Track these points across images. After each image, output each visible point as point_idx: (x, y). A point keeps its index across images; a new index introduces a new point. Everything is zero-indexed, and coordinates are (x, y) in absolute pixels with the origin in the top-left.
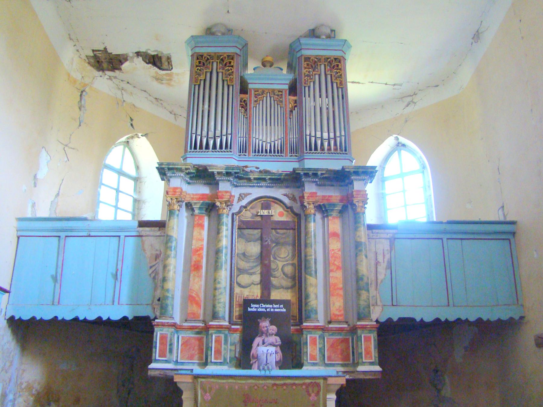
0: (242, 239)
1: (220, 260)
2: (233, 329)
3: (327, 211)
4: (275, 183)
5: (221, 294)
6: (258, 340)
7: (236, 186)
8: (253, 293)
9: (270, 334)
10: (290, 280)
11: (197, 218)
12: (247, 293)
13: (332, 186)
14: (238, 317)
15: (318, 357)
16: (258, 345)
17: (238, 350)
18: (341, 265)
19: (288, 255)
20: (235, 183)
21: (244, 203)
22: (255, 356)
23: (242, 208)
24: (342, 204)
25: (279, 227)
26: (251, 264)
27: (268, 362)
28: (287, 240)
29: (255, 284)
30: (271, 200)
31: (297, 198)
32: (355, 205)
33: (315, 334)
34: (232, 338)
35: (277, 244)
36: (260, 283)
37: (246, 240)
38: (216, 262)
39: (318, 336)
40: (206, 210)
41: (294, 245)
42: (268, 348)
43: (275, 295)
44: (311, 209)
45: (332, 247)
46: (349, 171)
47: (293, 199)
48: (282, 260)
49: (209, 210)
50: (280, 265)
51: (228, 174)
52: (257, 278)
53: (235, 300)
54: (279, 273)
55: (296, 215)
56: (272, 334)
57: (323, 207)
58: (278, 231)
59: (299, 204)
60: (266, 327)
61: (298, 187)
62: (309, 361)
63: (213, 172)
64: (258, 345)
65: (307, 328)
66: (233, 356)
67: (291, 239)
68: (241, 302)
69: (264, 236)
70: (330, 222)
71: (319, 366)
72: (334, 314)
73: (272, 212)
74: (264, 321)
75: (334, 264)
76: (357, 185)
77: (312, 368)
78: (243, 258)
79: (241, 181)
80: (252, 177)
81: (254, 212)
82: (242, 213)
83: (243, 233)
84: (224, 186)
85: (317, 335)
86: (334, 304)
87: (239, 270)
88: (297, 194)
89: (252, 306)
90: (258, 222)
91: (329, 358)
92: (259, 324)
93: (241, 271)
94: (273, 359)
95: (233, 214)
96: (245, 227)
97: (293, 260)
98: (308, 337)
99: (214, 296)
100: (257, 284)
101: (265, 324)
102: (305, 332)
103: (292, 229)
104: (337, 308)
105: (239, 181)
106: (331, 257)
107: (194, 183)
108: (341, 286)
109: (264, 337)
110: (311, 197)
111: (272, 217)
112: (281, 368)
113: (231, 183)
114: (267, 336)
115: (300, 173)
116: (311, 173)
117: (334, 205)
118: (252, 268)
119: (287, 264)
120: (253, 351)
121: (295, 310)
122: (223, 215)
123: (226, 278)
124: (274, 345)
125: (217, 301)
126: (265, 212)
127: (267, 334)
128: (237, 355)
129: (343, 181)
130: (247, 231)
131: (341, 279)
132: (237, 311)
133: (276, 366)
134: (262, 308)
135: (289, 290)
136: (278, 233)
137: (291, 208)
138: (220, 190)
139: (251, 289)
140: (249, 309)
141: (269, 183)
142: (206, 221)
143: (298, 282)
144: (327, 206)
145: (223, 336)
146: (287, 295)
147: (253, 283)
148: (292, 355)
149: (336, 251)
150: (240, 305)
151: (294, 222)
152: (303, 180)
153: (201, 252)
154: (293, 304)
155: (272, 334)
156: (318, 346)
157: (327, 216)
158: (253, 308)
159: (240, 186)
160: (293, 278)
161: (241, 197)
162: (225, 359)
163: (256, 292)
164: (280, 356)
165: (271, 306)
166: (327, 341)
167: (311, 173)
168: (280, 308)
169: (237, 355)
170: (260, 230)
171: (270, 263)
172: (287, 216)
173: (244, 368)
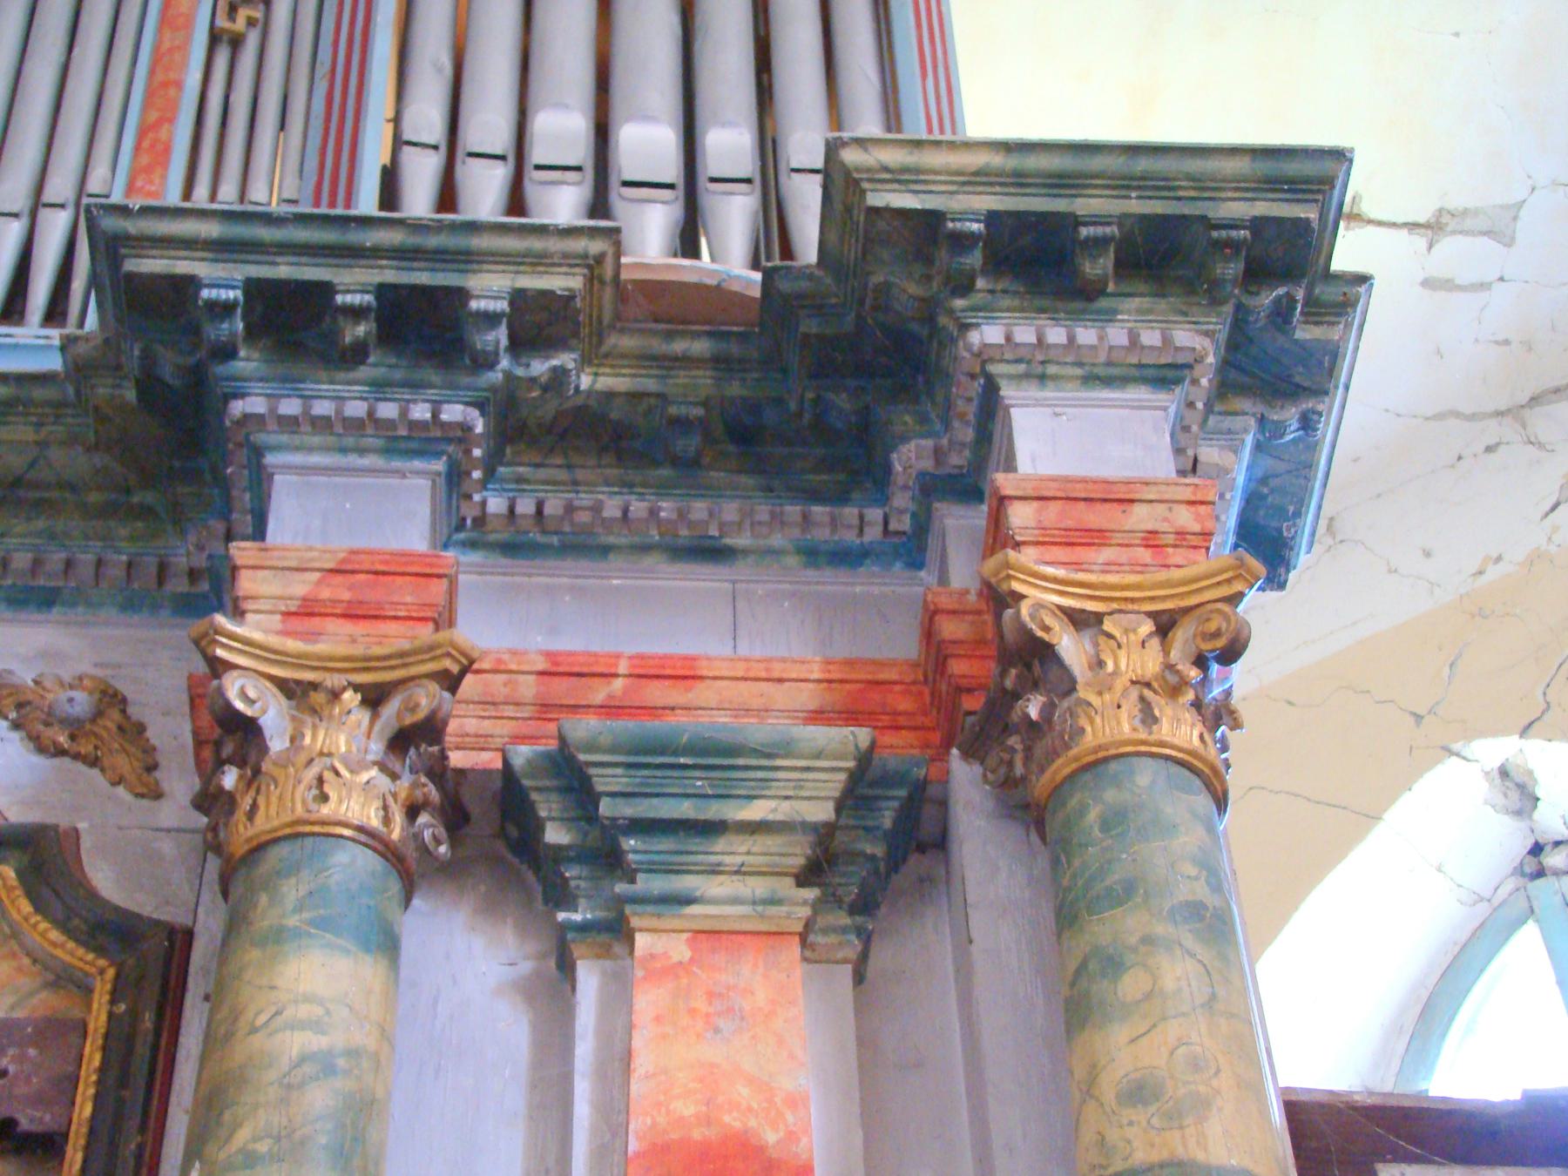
3: (607, 858)
13: (710, 551)
46: (931, 221)
57: (547, 806)
59: (177, 806)
70: (647, 1001)
76: (1062, 436)
110: (352, 614)
115: (189, 284)
116: (354, 285)
117: (719, 759)
129: (855, 464)
144: (604, 781)
151: (59, 1032)
152: (255, 404)
157: (614, 931)
167: (354, 285)
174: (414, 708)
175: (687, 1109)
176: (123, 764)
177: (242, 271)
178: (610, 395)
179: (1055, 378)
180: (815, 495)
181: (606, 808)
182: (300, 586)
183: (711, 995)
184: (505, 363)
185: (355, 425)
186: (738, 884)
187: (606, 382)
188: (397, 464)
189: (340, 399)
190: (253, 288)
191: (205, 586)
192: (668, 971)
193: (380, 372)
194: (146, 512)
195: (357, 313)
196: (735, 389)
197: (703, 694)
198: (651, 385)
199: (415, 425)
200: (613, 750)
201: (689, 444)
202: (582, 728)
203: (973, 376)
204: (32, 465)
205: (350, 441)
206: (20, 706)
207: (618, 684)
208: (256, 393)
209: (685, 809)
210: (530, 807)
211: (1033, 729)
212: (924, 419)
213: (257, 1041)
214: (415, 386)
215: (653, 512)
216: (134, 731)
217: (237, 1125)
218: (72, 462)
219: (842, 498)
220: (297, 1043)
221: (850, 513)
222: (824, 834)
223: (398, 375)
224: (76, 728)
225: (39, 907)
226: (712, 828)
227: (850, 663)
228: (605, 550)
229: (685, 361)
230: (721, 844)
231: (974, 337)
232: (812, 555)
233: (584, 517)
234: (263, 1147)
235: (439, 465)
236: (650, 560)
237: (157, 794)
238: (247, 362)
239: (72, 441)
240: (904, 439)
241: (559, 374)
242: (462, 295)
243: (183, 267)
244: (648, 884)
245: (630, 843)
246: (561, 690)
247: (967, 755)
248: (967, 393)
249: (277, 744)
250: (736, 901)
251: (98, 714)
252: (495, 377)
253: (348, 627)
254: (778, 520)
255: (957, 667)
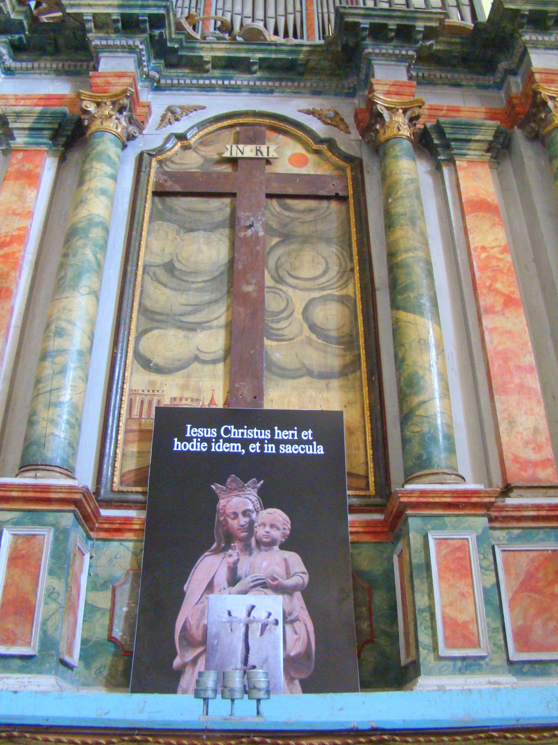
0: (165, 224)
1: (72, 260)
2: (109, 520)
3: (447, 146)
4: (280, 80)
5: (63, 371)
6: (210, 566)
7: (158, 88)
8: (199, 390)
9: (259, 543)
10: (335, 349)
11: (20, 156)
12: (172, 391)
13: (457, 85)
14: (131, 477)
15: (483, 627)
16: (210, 587)
17: (122, 609)
18: (517, 295)
19: (325, 272)
20: (153, 73)
21: (179, 127)
22: (197, 633)
23: (173, 140)
24: (498, 123)
25: (290, 191)
26: (194, 298)
27: (252, 660)
28: (320, 227)
29: (204, 362)
30: (267, 121)
31: (350, 120)
32: (544, 104)
33: (455, 528)
34: (103, 560)
35: (287, 238)
36: (225, 358)
37: (181, 227)
38: (62, 266)
39: (472, 539)
40: (55, 137)
41: (345, 242)
42: (251, 599)
43: (279, 396)
44: (399, 126)
45: (476, 240)
47: (335, 121)
48: (308, 289)
49: (63, 140)
50: (299, 300)
51: (129, 24)
52: (214, 341)
53: (124, 412)
54: (294, 326)
55: (348, 158)
56: (271, 544)
57: (434, 136)
58: (289, 202)
60: (246, 513)
61: (351, 94)
62: (443, 651)
63: (81, 15)
64: (210, 587)
65: (425, 504)
66: (101, 633)
67: (335, 225)
68: (149, 423)
69: (241, 214)
70: (461, 174)
71: (494, 670)
72: (516, 460)
73: (270, 149)
74: (241, 489)
75: (497, 291)
77: (456, 682)
78: (164, 276)
79: (173, 72)
80: (207, 55)
81: (212, 152)
82: (169, 153)
83: (171, 210)
84: (117, 65)
85: (470, 528)
86: (512, 423)
87: (144, 311)
88: (347, 109)
89: (190, 431)
90: (226, 175)
91: (524, 639)
92: (216, 499)
93: (154, 318)
94: (274, 649)
95: (141, 155)
96: (178, 188)
97: (345, 285)
98: (434, 539)
99: (38, 381)
100: (214, 362)
101: (239, 502)
102: (414, 523)
103: (338, 198)
104: (527, 435)
105: (165, 72)
106: (483, 269)
107: (26, 72)
108: (529, 359)
109: (234, 554)
110: (397, 94)
111: (267, 167)
112: (308, 687)
113: (140, 64)
114: (247, 549)
115: (357, 24)
116: (392, 24)
117: (470, 126)
118: (197, 308)
119: (325, 299)
120: (187, 614)
121: (358, 454)
122: (103, 136)
123: (93, 323)
124: (279, 589)
125: (43, 399)
126: (249, 151)
127: (250, 541)
128: (118, 633)
129: (489, 67)
130: (182, 204)
131: (527, 337)
132: (129, 456)
133: (290, 679)
134: (228, 442)
135: (335, 383)
136: (288, 208)
137: (331, 143)
138: (100, 70)
139: (189, 376)
140: (178, 446)
141: (260, 79)
142: (48, 168)
143: (370, 350)
144: (447, 130)
145: (47, 535)
146: (327, 398)
147: (196, 358)
148: (359, 632)
149: (493, 252)
150: (143, 433)
152: (370, 50)
153: (15, 247)
154: (351, 433)
155: (272, 543)
156: (480, 580)
157: (451, 161)
158: (194, 441)
159: (171, 88)
160: (348, 342)
161: (172, 114)
162: (48, 644)
163: (210, 388)
164: (302, 635)
165: (266, 434)
166: (506, 564)
167: (392, 24)
168: (300, 442)
169: (118, 633)
170: (227, 200)
171: (261, 287)
172: (318, 165)
173: (140, 687)
174: (415, 113)
175: (473, 194)
176: (341, 126)
177: (369, 21)
178: (439, 50)
179: (539, 48)
180: (480, 74)
181: (447, 136)
182: (386, 88)
183: (473, 173)
184: (421, 42)
185: (390, 55)
186: (474, 152)
187: (438, 48)
188: (399, 63)
189: (387, 49)
190: (371, 24)
191: (351, 91)
192: (464, 168)
193: (395, 44)
194: (339, 75)
195: (392, 30)
196: (465, 50)
197: (462, 114)
198: (447, 48)
199: (402, 55)
200: (449, 124)
201: (454, 62)
202: (442, 120)
203: (521, 47)
204: (317, 64)
205: (389, 59)
206: (319, 115)
207: (444, 112)
208: (370, 48)
209: (463, 137)
210: (430, 136)
211: (542, 120)
212: (506, 57)
213: (398, 176)
214: (403, 47)
215: (447, 76)
216: (342, 120)
217: (398, 191)
218: (325, 64)
219: (484, 74)
220: (405, 177)
221: (487, 78)
222: (490, 143)
223: (399, 44)
224: (331, 118)
225: (333, 154)
226: (468, 141)
227: (491, 109)
228: (436, 84)
229: (455, 43)
230: (470, 144)
231: (523, 38)
232: (479, 87)
233: (432, 77)
234: (404, 195)
235: (407, 64)
236: (445, 87)
237: (349, 133)
238: (368, 41)
239: (325, 59)
240: (501, 61)
241: (431, 45)
242: (414, 27)
243: (357, 20)
244: (455, 151)
245: (452, 143)
246: (432, 112)
247: (519, 127)
248: (518, 51)
249: (387, 119)
250: (475, 155)
251: (335, 117)
252: (419, 45)
253: (397, 97)
254: (472, 79)
255: (517, 109)
